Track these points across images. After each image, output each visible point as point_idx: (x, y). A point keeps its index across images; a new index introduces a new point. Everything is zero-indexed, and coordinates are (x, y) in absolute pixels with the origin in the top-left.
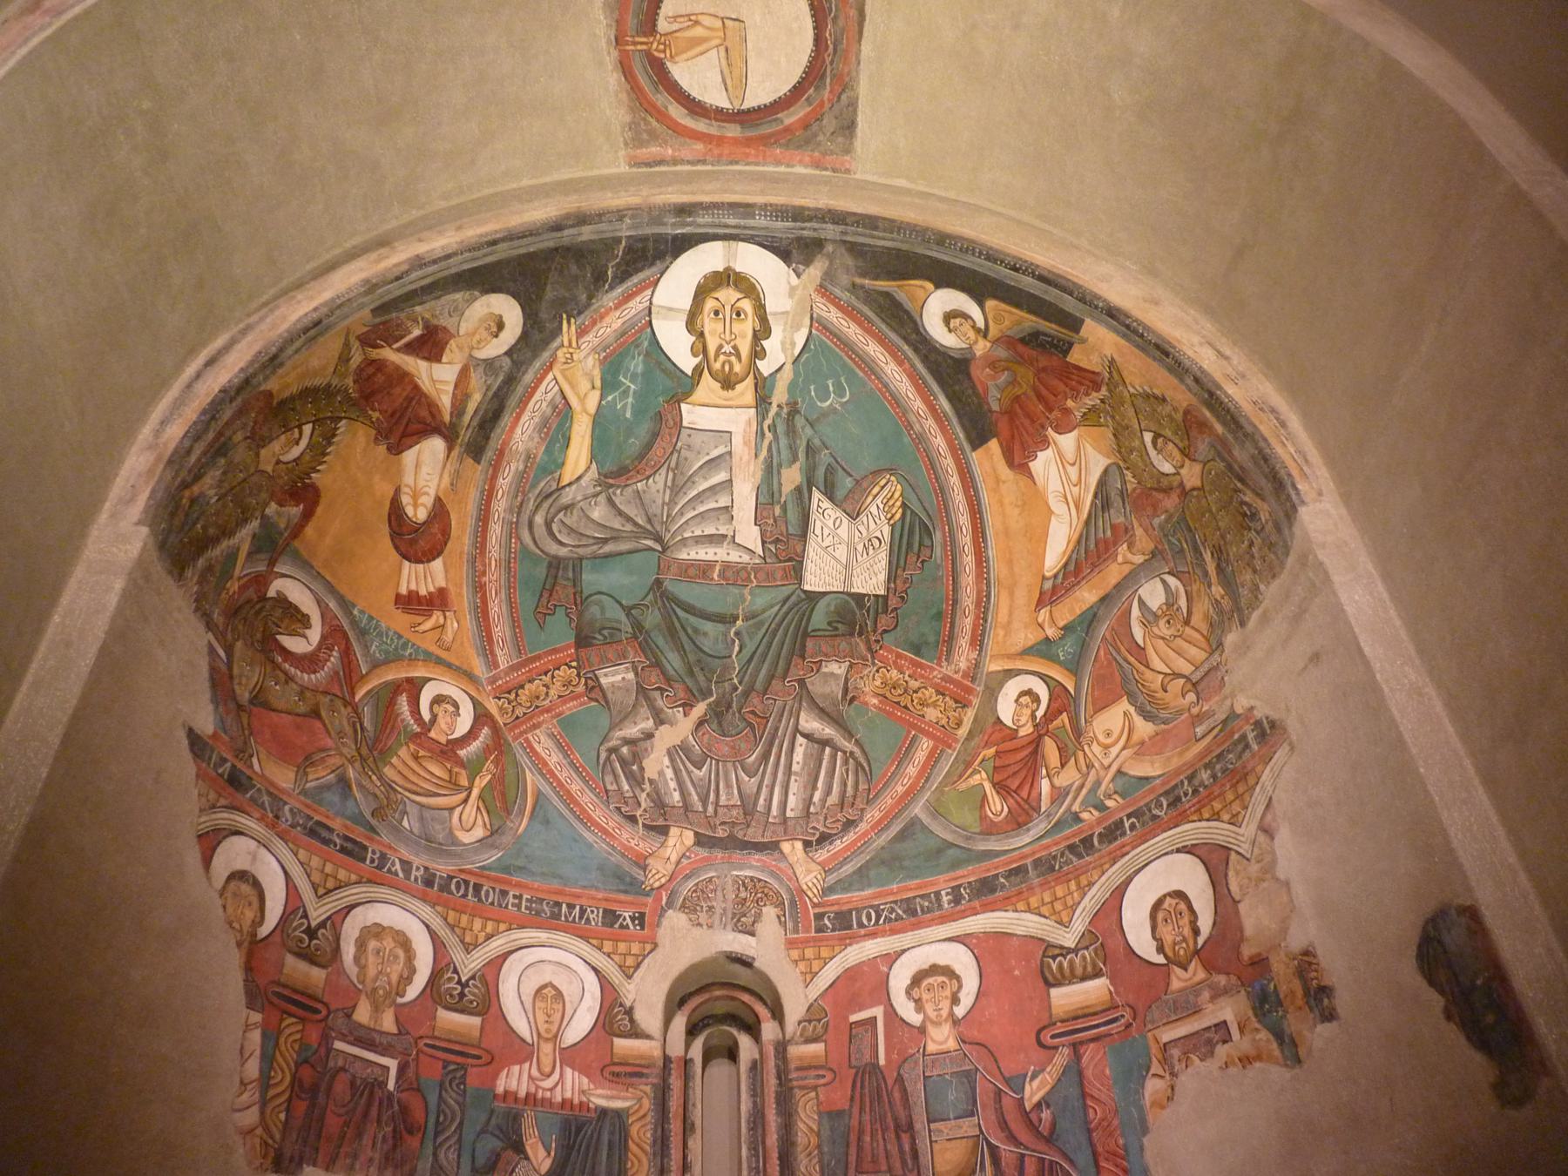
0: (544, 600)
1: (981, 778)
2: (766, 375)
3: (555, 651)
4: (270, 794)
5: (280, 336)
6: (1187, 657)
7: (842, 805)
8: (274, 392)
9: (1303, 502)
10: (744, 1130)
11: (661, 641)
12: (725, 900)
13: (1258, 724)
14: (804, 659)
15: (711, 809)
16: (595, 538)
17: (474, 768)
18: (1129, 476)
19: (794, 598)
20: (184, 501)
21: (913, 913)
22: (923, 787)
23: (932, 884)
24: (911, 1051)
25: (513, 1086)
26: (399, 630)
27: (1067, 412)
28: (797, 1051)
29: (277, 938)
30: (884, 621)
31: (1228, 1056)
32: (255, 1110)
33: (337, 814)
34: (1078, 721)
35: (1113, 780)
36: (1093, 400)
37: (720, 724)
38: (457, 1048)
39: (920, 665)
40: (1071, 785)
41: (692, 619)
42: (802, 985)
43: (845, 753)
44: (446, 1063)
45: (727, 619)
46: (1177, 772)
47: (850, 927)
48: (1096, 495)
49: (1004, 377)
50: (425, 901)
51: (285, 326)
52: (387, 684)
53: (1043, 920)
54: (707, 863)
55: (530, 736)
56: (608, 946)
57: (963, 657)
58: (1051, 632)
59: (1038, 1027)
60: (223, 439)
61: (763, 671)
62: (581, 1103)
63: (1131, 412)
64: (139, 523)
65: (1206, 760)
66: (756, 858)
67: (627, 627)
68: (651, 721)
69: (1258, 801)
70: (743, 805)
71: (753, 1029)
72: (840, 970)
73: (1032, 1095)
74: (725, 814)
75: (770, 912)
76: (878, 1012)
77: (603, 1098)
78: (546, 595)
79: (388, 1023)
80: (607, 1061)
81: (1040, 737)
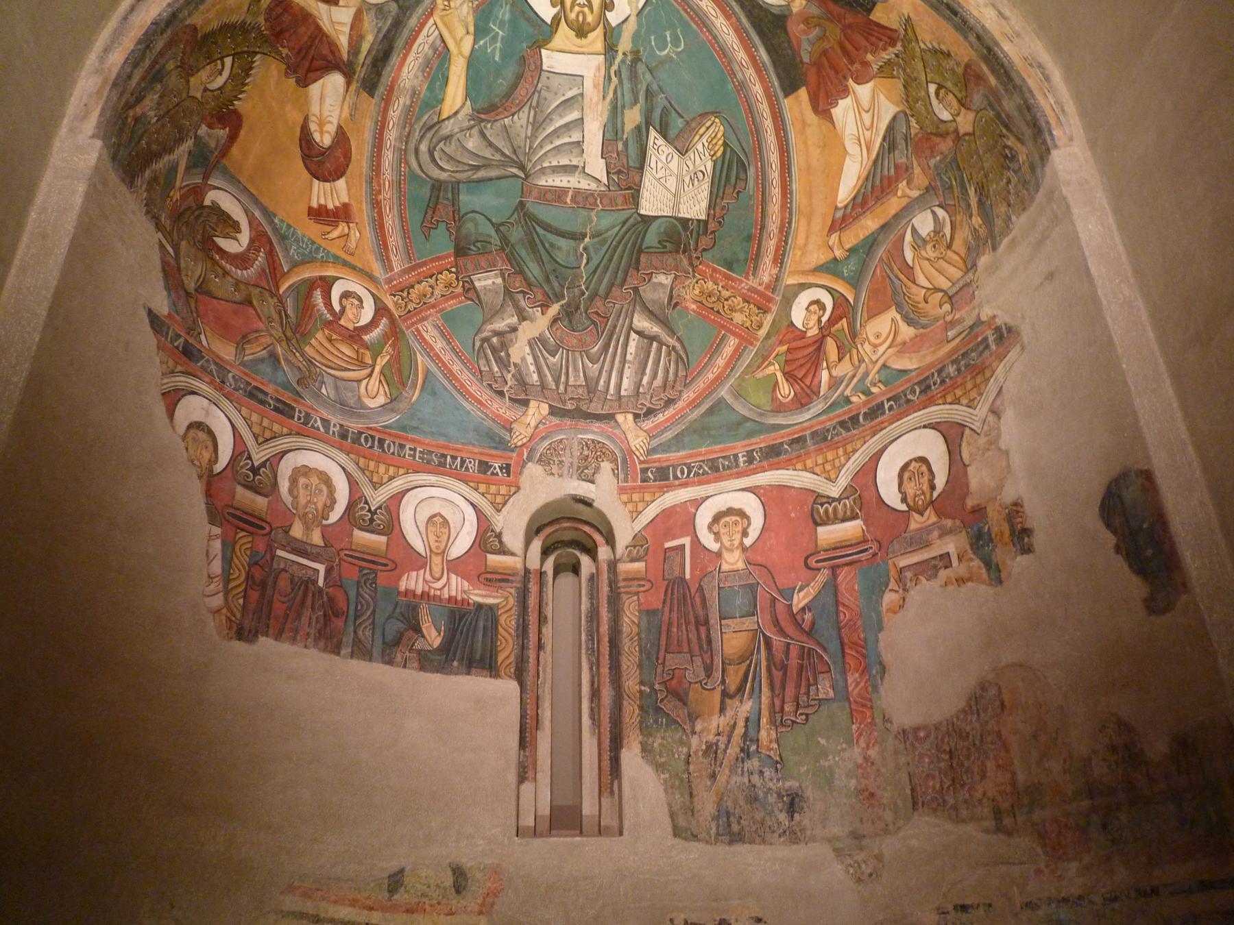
0: (429, 216)
1: (774, 369)
2: (614, 24)
3: (439, 259)
4: (216, 364)
7: (664, 386)
8: (198, 26)
9: (1056, 146)
10: (583, 622)
11: (523, 253)
13: (998, 329)
14: (638, 271)
15: (562, 388)
16: (469, 165)
18: (913, 122)
19: (632, 221)
20: (129, 120)
21: (717, 470)
22: (729, 375)
23: (732, 448)
24: (710, 569)
25: (412, 586)
26: (312, 237)
27: (866, 64)
28: (623, 567)
29: (229, 473)
30: (705, 241)
31: (949, 577)
32: (221, 595)
33: (270, 381)
34: (854, 326)
36: (888, 54)
37: (570, 322)
38: (369, 557)
39: (733, 280)
40: (846, 375)
41: (551, 237)
42: (629, 520)
43: (668, 346)
44: (361, 569)
45: (577, 237)
46: (929, 367)
47: (667, 479)
48: (884, 139)
49: (816, 32)
50: (341, 450)
52: (304, 281)
53: (815, 477)
54: (559, 429)
56: (482, 488)
57: (767, 272)
58: (838, 253)
59: (805, 555)
60: (157, 67)
61: (605, 281)
62: (463, 600)
63: (920, 66)
64: (93, 137)
65: (954, 357)
67: (496, 240)
68: (516, 317)
69: (992, 388)
70: (587, 385)
71: (592, 552)
72: (659, 510)
73: (799, 602)
74: (573, 392)
75: (606, 466)
76: (686, 541)
77: (479, 596)
78: (430, 213)
79: (316, 538)
80: (483, 570)
81: (824, 337)
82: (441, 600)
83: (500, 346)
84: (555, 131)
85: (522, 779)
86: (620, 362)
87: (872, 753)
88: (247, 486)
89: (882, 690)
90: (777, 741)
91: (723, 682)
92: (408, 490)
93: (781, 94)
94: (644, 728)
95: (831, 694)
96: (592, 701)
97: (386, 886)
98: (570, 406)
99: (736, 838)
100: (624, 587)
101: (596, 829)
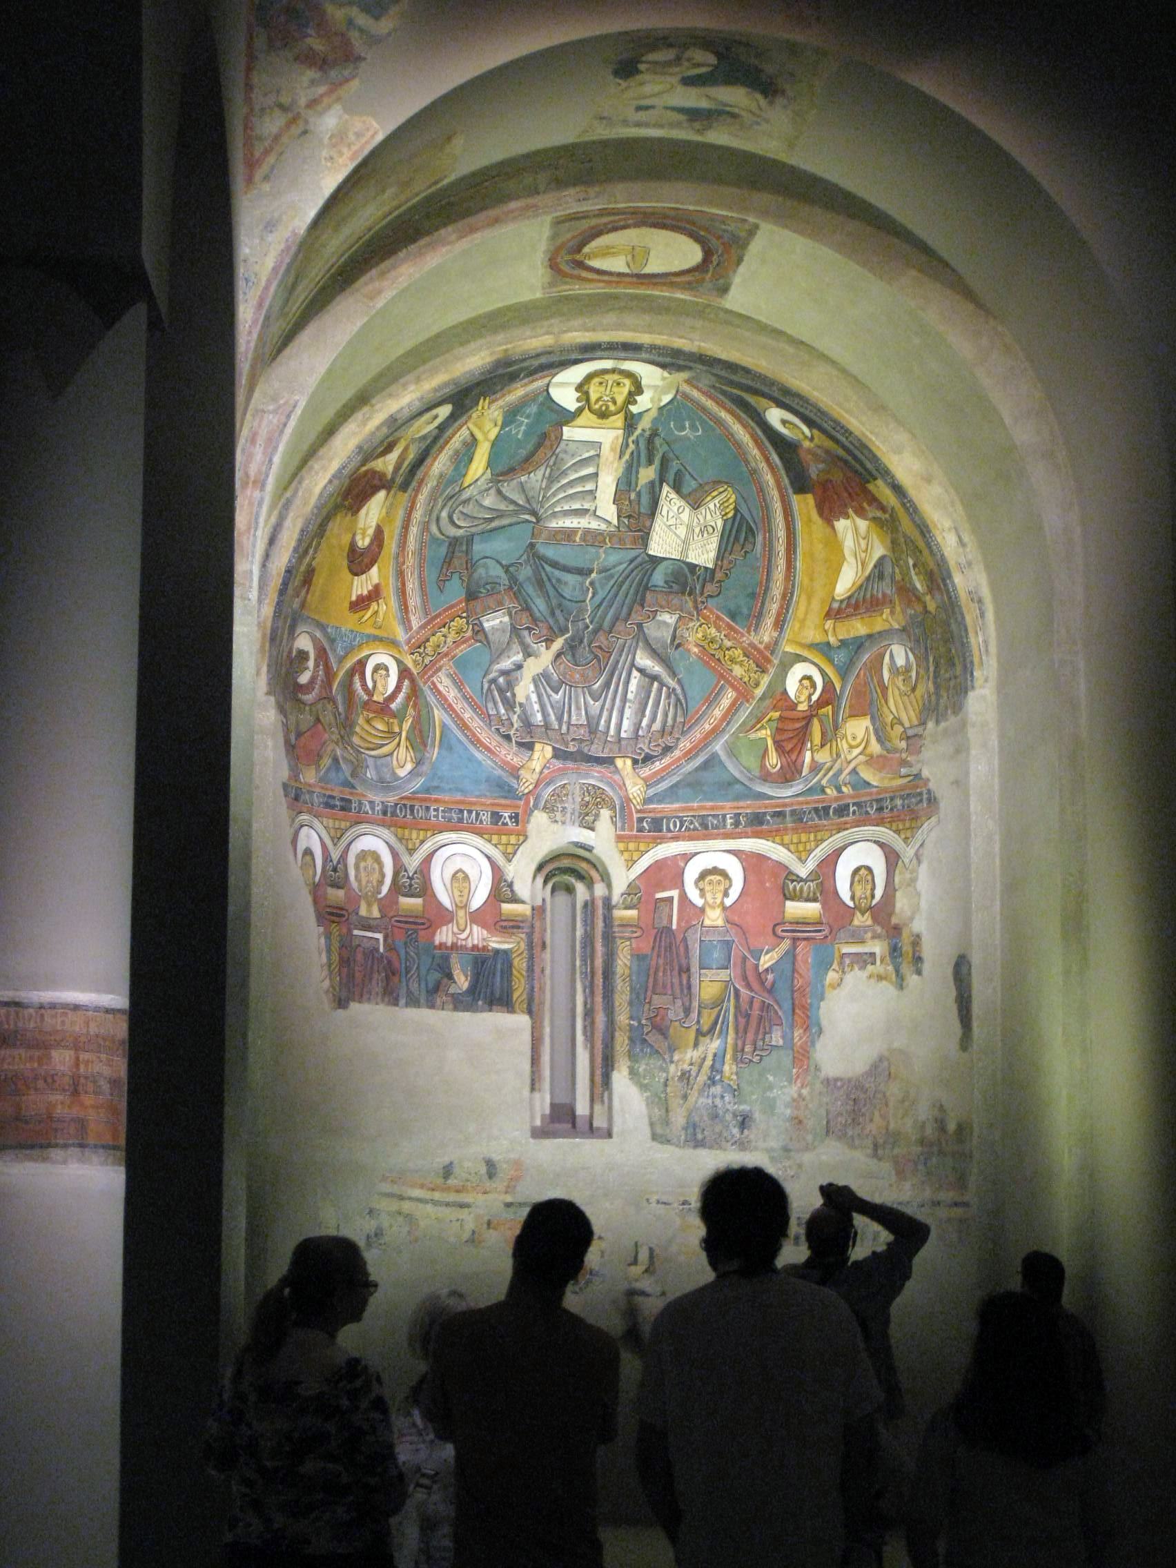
0: (444, 570)
1: (766, 733)
3: (452, 607)
5: (312, 513)
6: (909, 716)
7: (663, 731)
12: (574, 802)
13: (929, 792)
14: (643, 607)
15: (564, 728)
17: (400, 716)
18: (897, 570)
19: (639, 559)
21: (706, 827)
23: (722, 808)
25: (444, 940)
27: (862, 508)
28: (620, 914)
30: (710, 588)
34: (837, 719)
35: (849, 774)
36: (879, 514)
37: (573, 656)
39: (736, 631)
41: (557, 573)
42: (624, 869)
43: (669, 688)
45: (584, 572)
46: (885, 790)
47: (661, 831)
48: (875, 566)
49: (821, 466)
51: (313, 500)
52: (347, 672)
53: (789, 854)
54: (562, 772)
55: (434, 679)
56: (495, 839)
57: (766, 634)
58: (832, 640)
64: (268, 693)
66: (597, 770)
67: (504, 579)
68: (521, 654)
69: (920, 835)
71: (590, 885)
72: (651, 861)
73: (765, 963)
74: (575, 732)
75: (605, 814)
76: (675, 893)
77: (497, 943)
79: (376, 913)
81: (812, 716)
82: (466, 948)
83: (505, 689)
84: (569, 483)
85: (533, 1089)
86: (621, 700)
87: (805, 1092)
88: (332, 886)
89: (818, 1046)
90: (737, 1074)
91: (698, 1022)
92: (436, 851)
93: (790, 491)
94: (631, 1056)
95: (781, 1042)
96: (585, 1020)
97: (441, 1175)
98: (572, 748)
99: (699, 1144)
100: (619, 932)
101: (587, 1127)
